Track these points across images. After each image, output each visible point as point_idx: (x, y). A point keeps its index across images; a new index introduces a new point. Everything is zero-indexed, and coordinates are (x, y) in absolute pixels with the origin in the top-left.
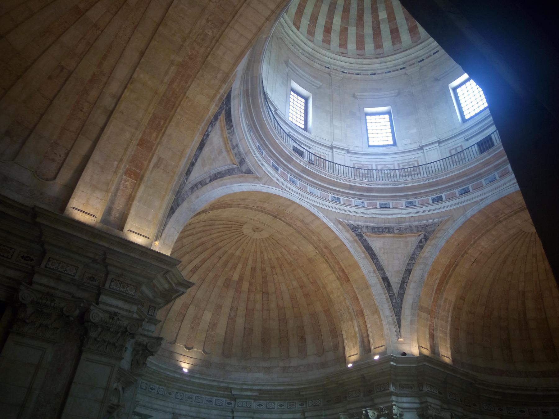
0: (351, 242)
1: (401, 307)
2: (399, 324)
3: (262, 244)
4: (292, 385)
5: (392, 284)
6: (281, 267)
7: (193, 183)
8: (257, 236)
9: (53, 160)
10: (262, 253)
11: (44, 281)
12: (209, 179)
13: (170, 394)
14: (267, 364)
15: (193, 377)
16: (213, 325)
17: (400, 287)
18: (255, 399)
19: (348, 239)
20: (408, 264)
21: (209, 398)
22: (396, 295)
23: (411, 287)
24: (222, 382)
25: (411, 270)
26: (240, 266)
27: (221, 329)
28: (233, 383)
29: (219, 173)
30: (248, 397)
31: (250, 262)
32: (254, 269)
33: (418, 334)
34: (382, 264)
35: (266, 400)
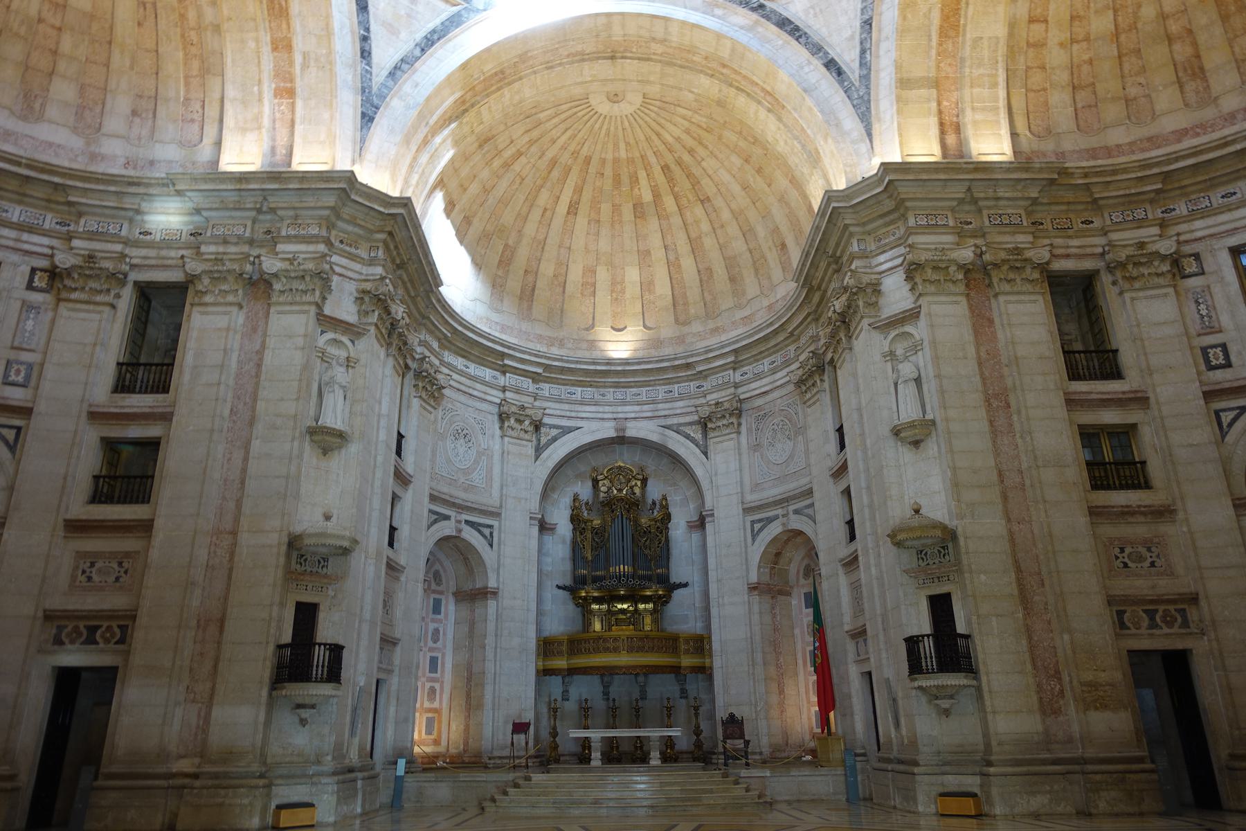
0: (750, 29)
1: (869, 101)
2: (870, 135)
3: (647, 119)
4: (771, 324)
5: (844, 68)
6: (701, 143)
7: (389, 65)
8: (625, 108)
9: (192, 121)
10: (658, 135)
11: (212, 249)
12: (418, 49)
13: (603, 395)
14: (747, 312)
15: (628, 364)
16: (647, 286)
17: (861, 64)
18: (735, 366)
19: (742, 28)
20: (863, 10)
21: (667, 388)
22: (857, 84)
23: (882, 53)
24: (675, 359)
25: (871, 18)
26: (642, 174)
27: (663, 288)
28: (692, 356)
29: (434, 31)
30: (723, 368)
31: (653, 159)
32: (665, 169)
33: (900, 135)
34: (816, 38)
35: (750, 364)
